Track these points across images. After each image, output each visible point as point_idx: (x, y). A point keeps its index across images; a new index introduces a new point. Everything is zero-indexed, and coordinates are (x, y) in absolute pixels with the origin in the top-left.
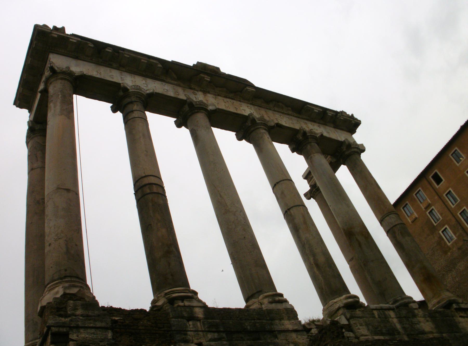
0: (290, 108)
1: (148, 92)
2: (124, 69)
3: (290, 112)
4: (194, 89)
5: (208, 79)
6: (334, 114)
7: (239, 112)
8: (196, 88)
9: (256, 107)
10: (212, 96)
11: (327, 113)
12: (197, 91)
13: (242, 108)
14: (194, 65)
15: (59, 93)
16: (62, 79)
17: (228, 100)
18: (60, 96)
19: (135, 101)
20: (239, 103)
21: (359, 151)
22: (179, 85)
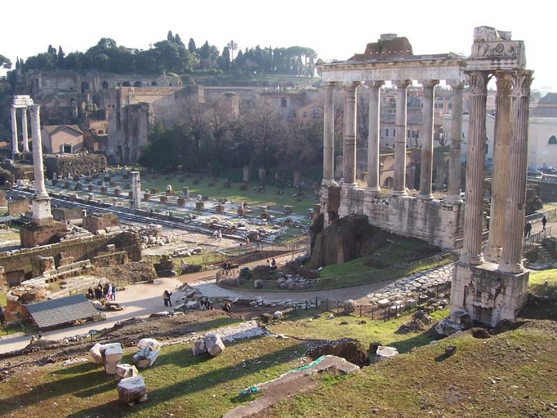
3: (419, 64)
14: (379, 40)
17: (386, 70)
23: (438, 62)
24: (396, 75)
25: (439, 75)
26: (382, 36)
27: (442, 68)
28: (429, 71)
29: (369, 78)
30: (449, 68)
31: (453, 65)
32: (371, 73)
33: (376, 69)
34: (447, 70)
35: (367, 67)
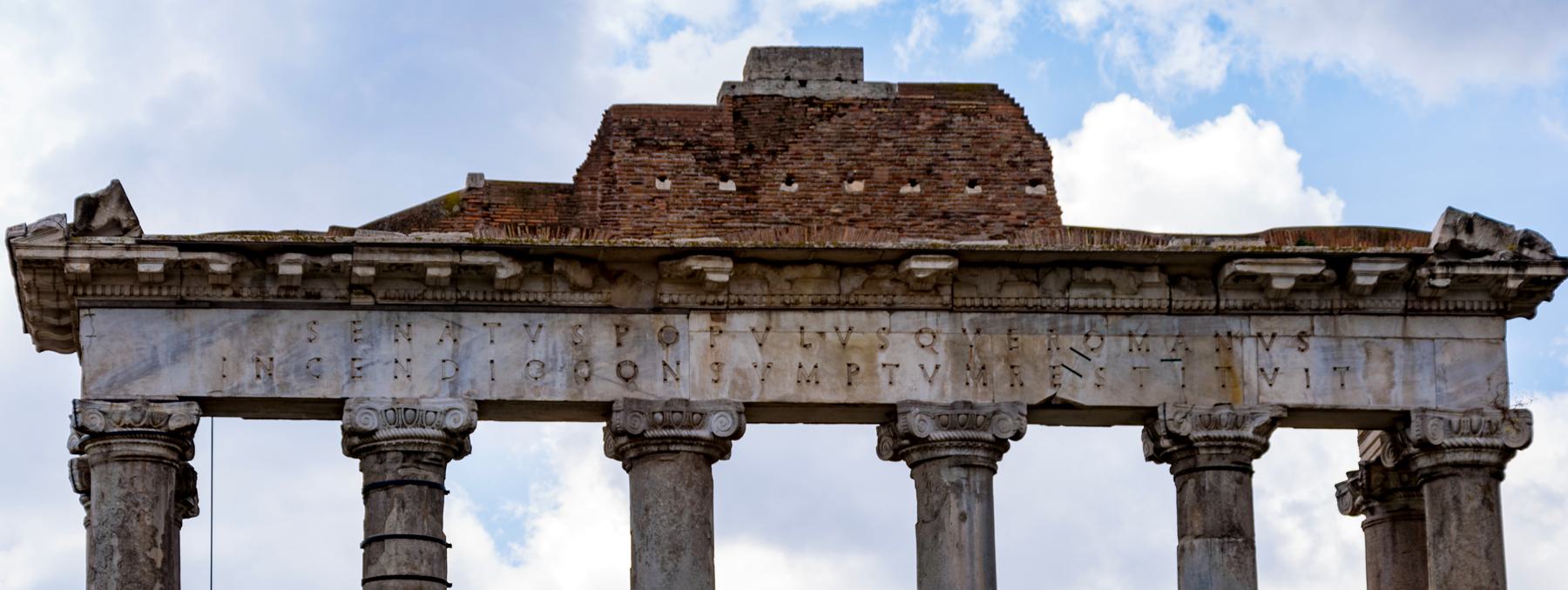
0: (1155, 277)
1: (452, 423)
2: (369, 301)
3: (1155, 295)
4: (675, 308)
5: (718, 272)
6: (1399, 266)
7: (861, 394)
8: (685, 299)
9: (967, 317)
10: (754, 319)
11: (1354, 275)
12: (687, 311)
13: (882, 357)
14: (731, 86)
15: (115, 542)
16: (123, 459)
17: (829, 319)
18: (117, 557)
19: (400, 483)
20: (883, 319)
21: (1484, 457)
22: (607, 309)
23: (1365, 275)
24: (943, 357)
25: (1340, 371)
26: (760, 57)
27: (1361, 327)
28: (1248, 353)
29: (653, 388)
30: (1418, 327)
31: (1460, 312)
32: (669, 338)
33: (718, 312)
34: (1407, 339)
35: (619, 294)
